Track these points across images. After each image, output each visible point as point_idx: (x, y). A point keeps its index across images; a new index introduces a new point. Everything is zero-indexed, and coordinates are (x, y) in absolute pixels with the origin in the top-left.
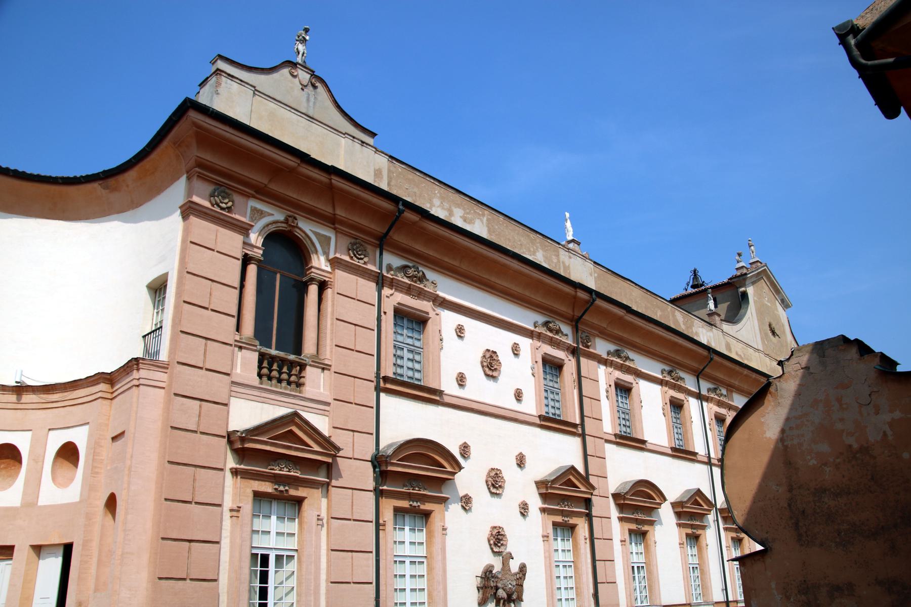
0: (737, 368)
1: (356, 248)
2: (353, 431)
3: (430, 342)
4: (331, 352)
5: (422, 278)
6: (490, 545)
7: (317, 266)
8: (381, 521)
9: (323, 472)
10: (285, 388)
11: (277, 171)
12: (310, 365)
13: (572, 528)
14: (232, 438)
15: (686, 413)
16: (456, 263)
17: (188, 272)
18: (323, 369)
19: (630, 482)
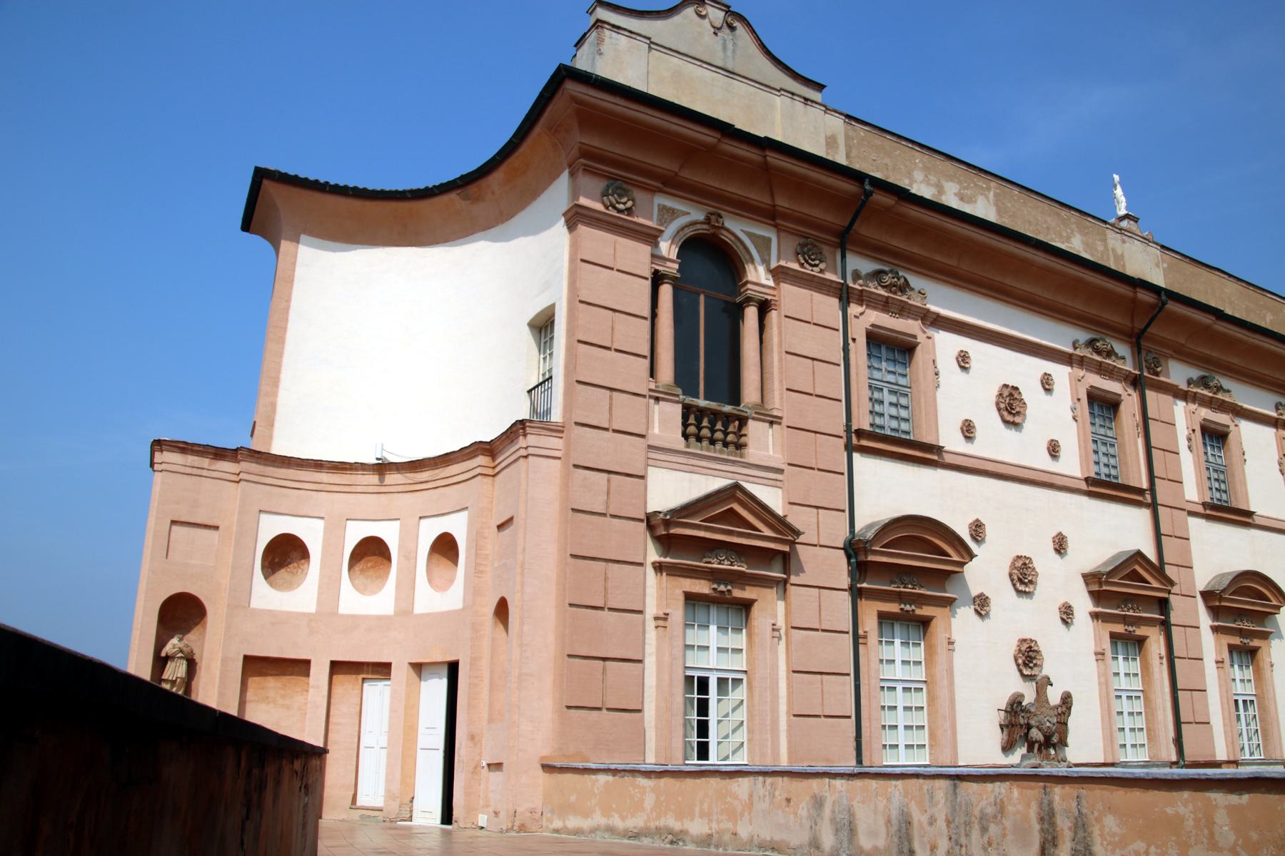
1: (808, 251)
2: (817, 507)
4: (781, 398)
5: (905, 287)
6: (1018, 665)
7: (754, 280)
8: (861, 632)
9: (778, 564)
10: (721, 452)
11: (689, 152)
12: (754, 419)
13: (1140, 642)
14: (653, 522)
16: (953, 262)
17: (581, 302)
18: (771, 423)
19: (1229, 574)
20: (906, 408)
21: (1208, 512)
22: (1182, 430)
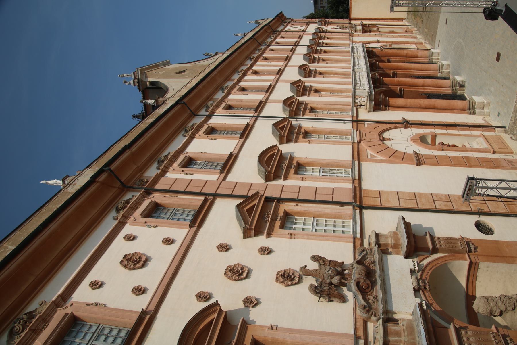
0: (196, 91)
3: (94, 316)
6: (292, 285)
13: (287, 215)
15: (218, 126)
16: (32, 279)
19: (258, 167)
20: (112, 330)
21: (225, 172)
22: (182, 176)
